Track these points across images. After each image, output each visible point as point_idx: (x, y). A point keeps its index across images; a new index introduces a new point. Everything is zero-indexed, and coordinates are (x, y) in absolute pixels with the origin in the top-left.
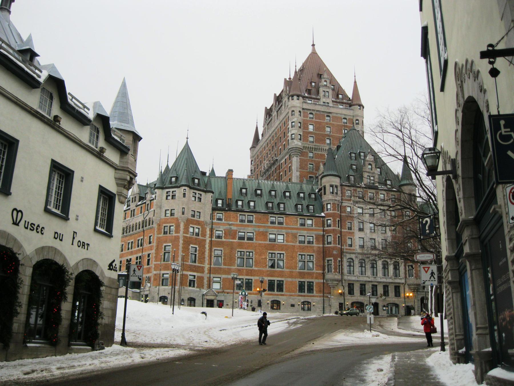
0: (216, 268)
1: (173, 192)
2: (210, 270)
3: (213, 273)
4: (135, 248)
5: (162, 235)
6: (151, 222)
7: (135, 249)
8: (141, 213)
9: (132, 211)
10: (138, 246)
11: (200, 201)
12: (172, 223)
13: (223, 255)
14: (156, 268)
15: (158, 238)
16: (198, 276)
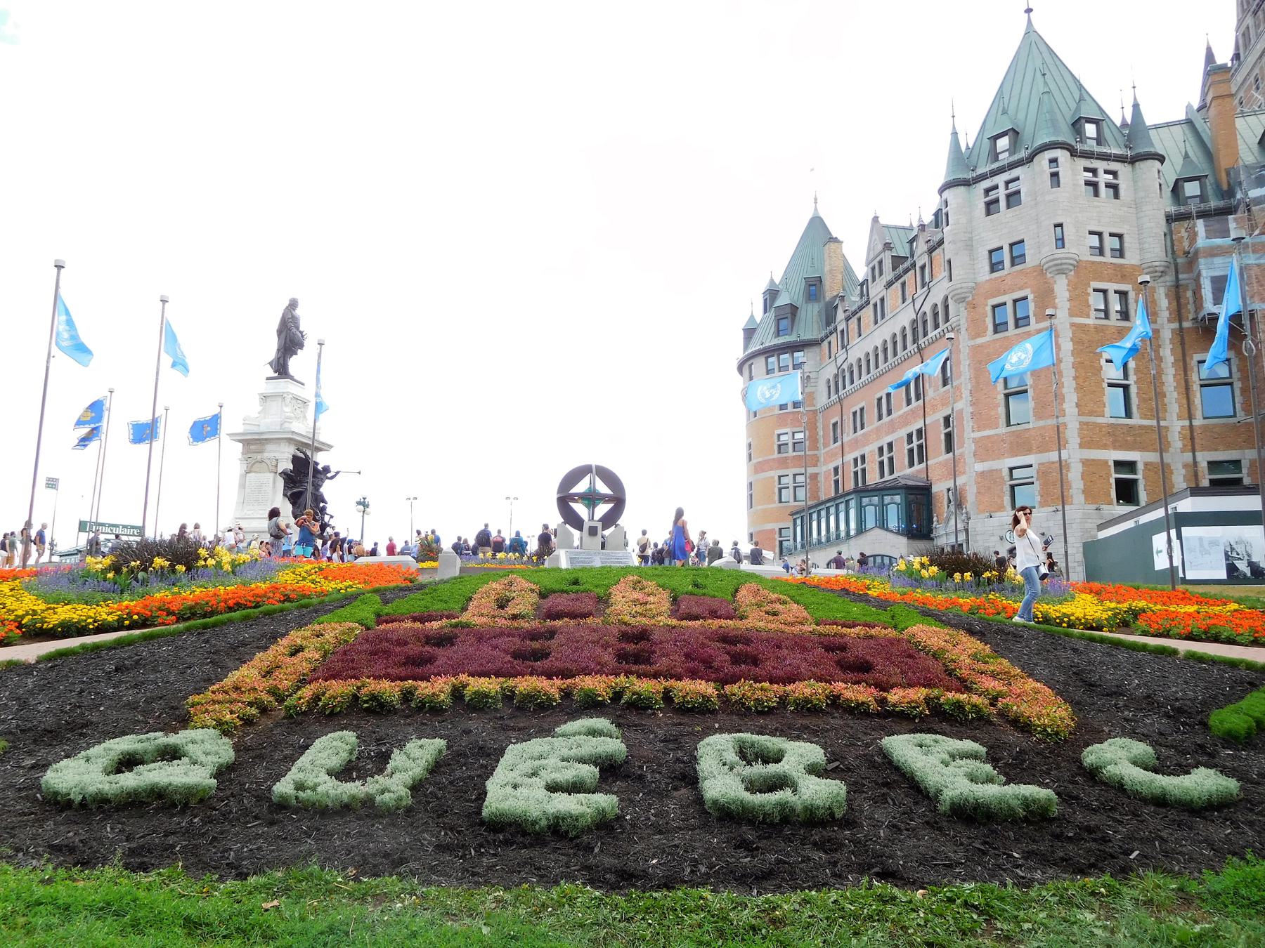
0: (1215, 426)
1: (1007, 183)
2: (1192, 438)
3: (1204, 449)
4: (900, 408)
5: (989, 335)
6: (941, 314)
7: (901, 412)
8: (904, 300)
9: (875, 305)
10: (909, 402)
11: (1117, 196)
12: (1020, 289)
13: (1236, 375)
14: (985, 450)
15: (975, 350)
16: (1146, 464)
